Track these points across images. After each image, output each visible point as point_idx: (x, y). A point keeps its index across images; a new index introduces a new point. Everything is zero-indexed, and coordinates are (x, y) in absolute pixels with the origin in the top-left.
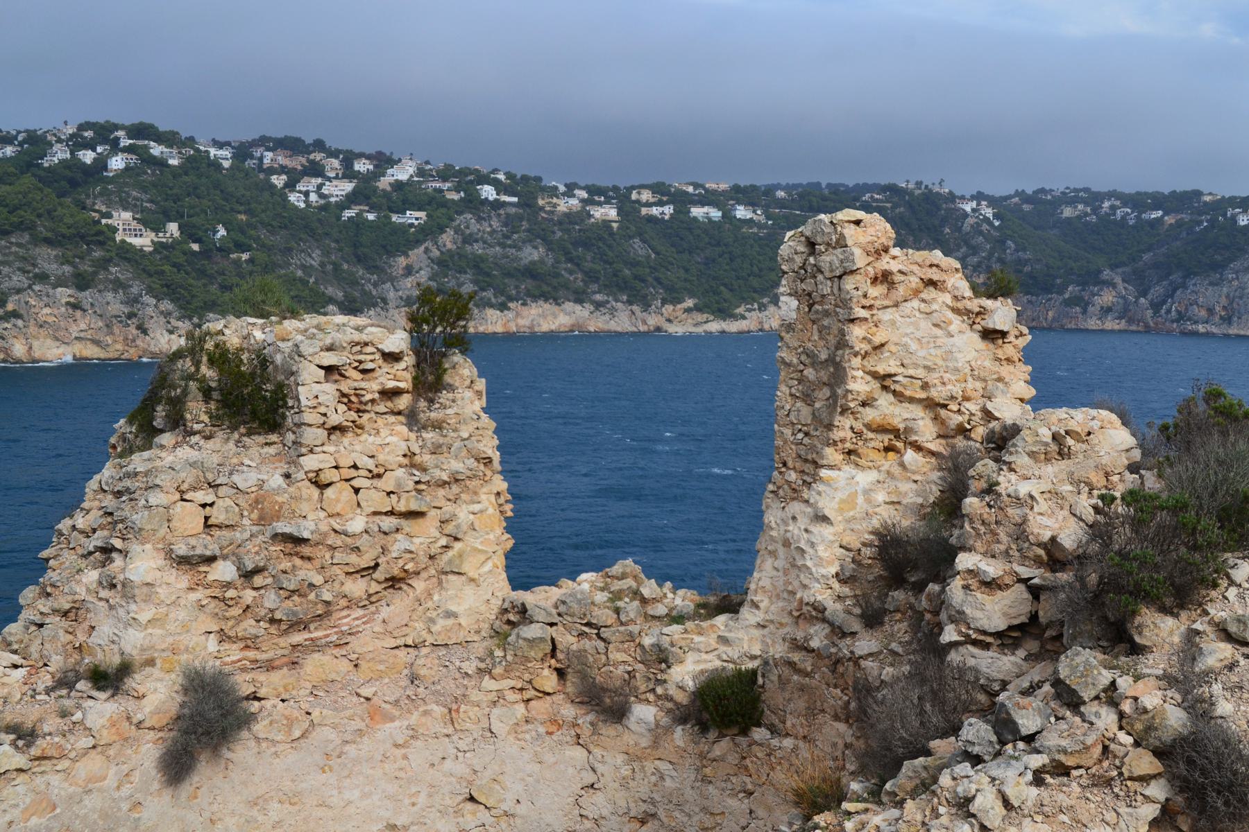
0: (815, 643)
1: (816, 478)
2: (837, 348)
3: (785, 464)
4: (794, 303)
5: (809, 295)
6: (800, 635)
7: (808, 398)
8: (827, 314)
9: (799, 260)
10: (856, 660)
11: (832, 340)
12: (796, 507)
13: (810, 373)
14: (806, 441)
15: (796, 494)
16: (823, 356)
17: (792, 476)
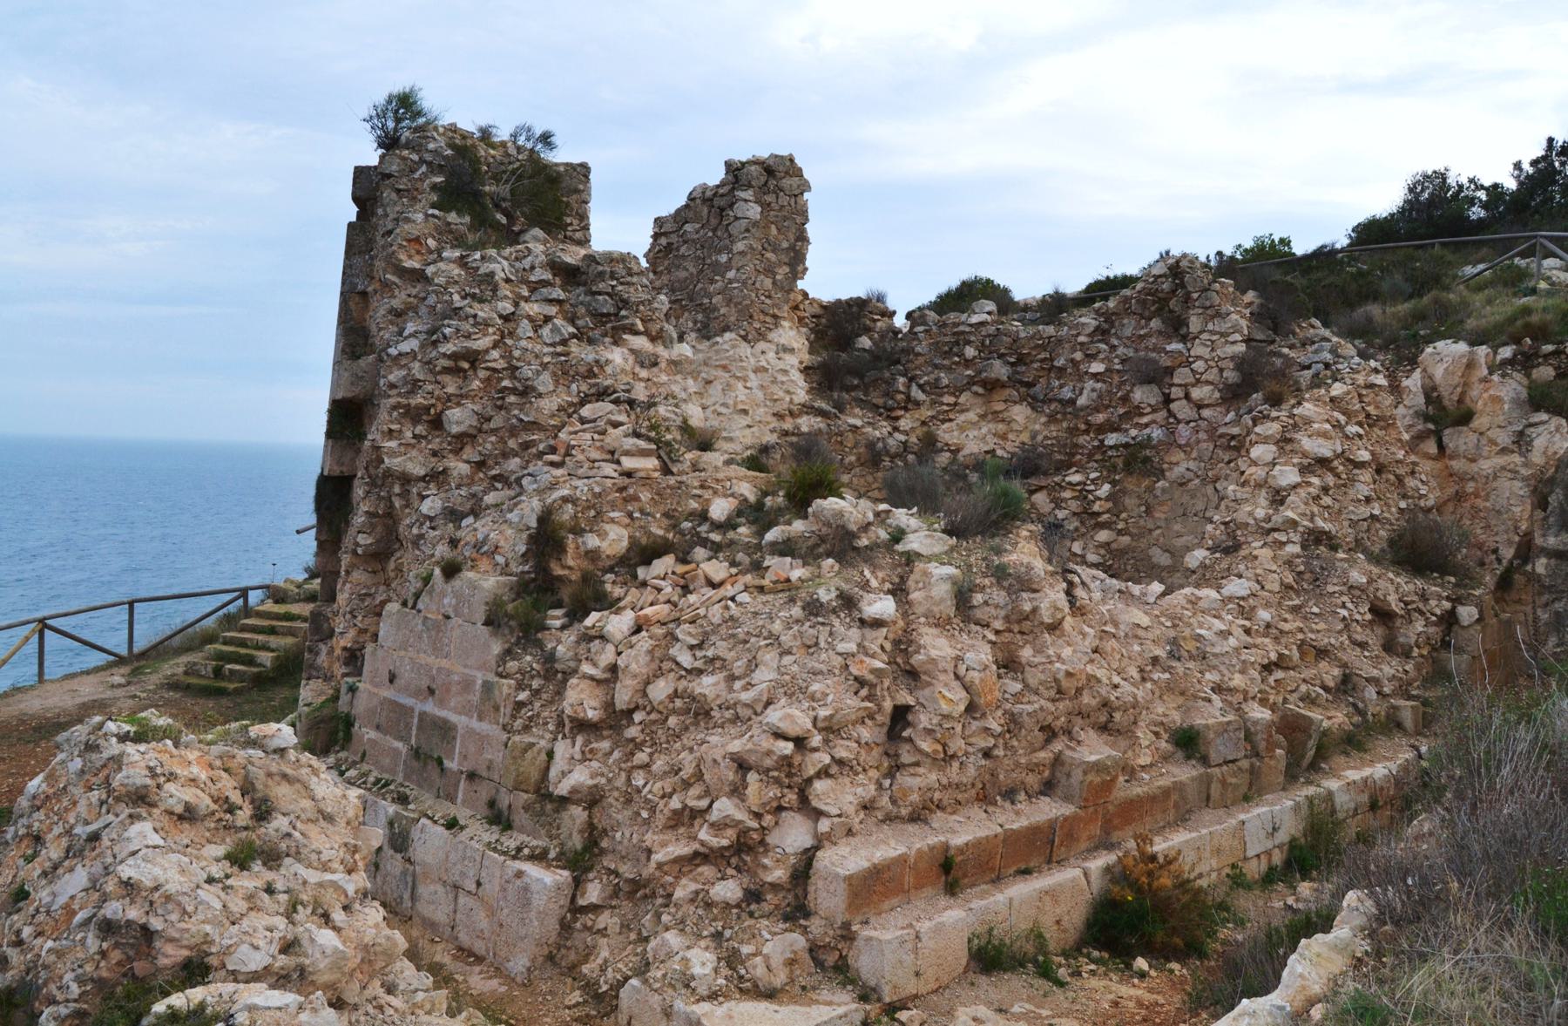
0: (805, 429)
1: (777, 325)
2: (797, 240)
3: (751, 317)
4: (759, 209)
5: (769, 204)
6: (788, 425)
7: (770, 271)
8: (785, 219)
9: (763, 179)
10: (854, 429)
11: (792, 237)
12: (761, 345)
13: (769, 255)
14: (768, 301)
15: (761, 336)
16: (785, 245)
17: (757, 325)
